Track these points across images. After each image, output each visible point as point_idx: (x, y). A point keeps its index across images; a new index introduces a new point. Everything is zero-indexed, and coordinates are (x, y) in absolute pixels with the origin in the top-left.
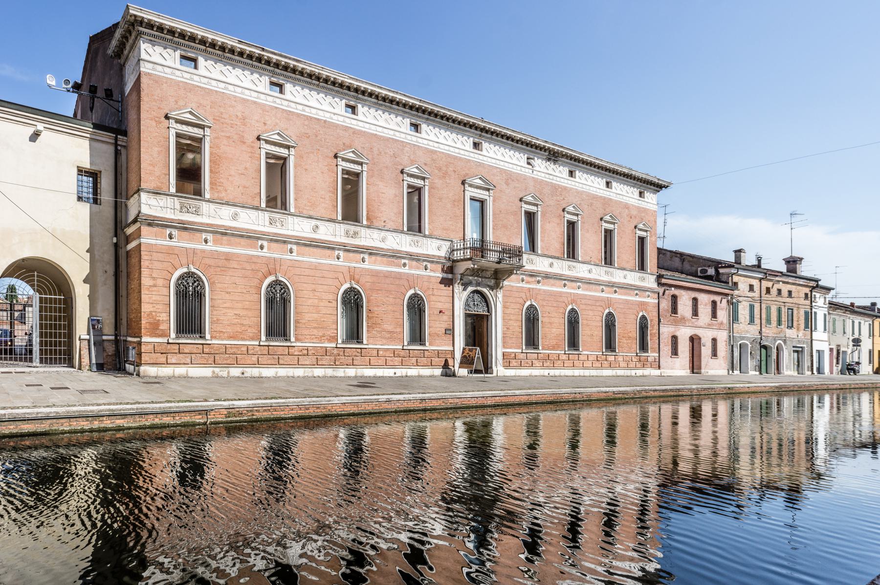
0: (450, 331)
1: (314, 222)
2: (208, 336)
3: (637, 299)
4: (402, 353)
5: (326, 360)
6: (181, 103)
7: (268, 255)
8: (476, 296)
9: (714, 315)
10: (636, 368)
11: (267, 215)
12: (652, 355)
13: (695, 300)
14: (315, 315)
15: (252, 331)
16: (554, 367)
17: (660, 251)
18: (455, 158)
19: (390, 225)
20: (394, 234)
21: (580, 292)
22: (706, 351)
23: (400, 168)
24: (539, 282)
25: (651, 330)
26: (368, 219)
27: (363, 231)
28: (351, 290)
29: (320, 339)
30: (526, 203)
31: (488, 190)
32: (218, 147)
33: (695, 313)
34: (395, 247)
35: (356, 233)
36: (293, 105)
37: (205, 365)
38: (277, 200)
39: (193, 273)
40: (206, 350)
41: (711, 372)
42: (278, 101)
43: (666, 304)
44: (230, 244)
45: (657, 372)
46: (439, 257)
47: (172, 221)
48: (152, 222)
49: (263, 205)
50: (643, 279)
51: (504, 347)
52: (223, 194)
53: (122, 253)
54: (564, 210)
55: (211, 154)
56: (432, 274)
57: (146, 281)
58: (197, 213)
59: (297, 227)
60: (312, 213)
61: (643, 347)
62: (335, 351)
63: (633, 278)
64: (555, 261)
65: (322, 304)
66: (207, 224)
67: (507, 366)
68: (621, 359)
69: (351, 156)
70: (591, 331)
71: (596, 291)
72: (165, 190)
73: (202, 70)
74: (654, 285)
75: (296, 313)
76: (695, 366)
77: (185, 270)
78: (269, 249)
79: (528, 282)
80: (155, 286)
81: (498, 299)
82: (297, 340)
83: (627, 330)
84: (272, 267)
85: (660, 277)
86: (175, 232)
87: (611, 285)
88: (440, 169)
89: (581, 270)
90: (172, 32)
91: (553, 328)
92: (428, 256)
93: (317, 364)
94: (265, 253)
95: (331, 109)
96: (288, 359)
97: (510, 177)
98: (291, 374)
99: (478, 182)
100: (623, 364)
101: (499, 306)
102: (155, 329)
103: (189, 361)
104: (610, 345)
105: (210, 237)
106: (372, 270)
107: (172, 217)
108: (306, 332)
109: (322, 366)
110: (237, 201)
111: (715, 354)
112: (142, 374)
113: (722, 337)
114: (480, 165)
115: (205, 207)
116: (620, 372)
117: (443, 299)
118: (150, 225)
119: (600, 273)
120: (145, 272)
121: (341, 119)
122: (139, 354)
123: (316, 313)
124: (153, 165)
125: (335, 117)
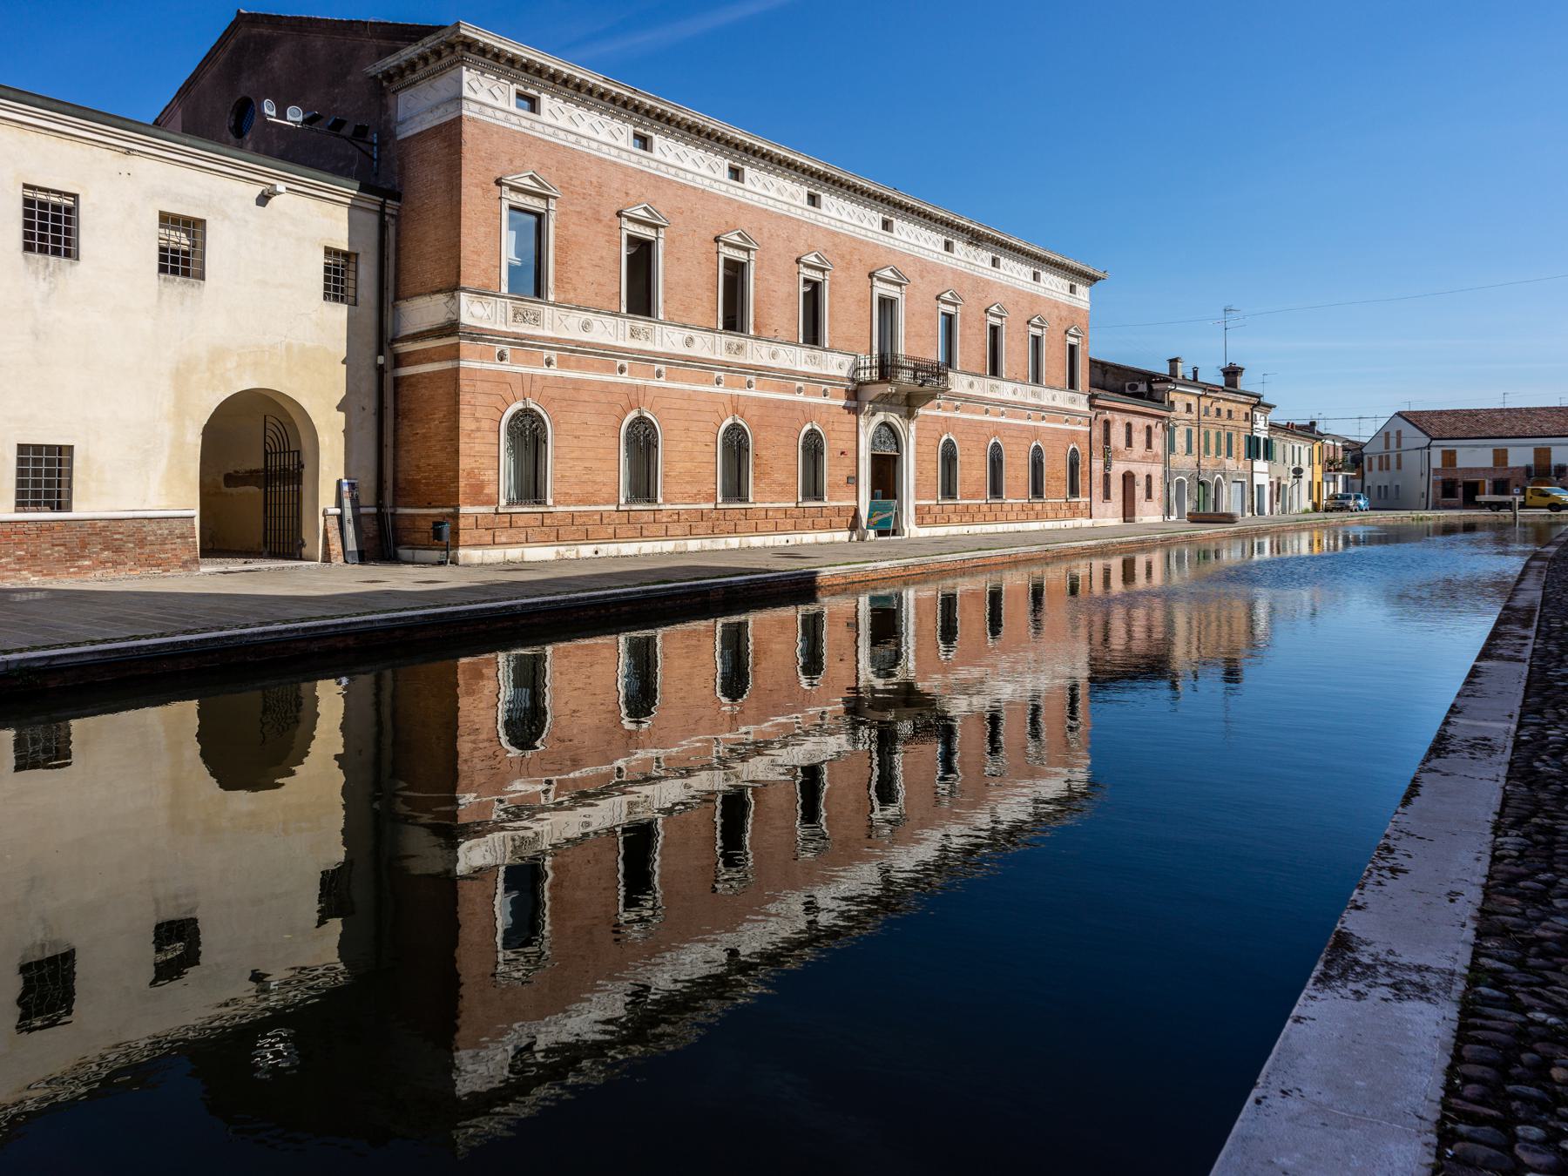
0: (854, 480)
1: (687, 333)
2: (550, 501)
3: (1067, 427)
4: (796, 512)
5: (703, 527)
6: (517, 163)
7: (629, 381)
8: (884, 430)
9: (1149, 445)
10: (1065, 518)
11: (628, 323)
12: (1083, 500)
13: (1129, 425)
14: (689, 465)
15: (606, 491)
16: (973, 522)
17: (1093, 363)
18: (862, 242)
19: (783, 335)
20: (788, 348)
21: (1003, 420)
22: (1140, 491)
23: (796, 256)
24: (957, 408)
25: (1083, 468)
26: (756, 327)
27: (749, 344)
28: (735, 427)
29: (695, 498)
30: (944, 302)
31: (900, 285)
32: (566, 227)
33: (1129, 443)
34: (787, 365)
35: (740, 347)
36: (663, 167)
37: (545, 542)
38: (641, 301)
39: (532, 410)
40: (548, 521)
41: (1147, 520)
42: (645, 161)
43: (1098, 433)
44: (579, 366)
45: (1087, 523)
46: (842, 378)
47: (506, 335)
48: (477, 335)
49: (624, 310)
50: (1073, 401)
51: (917, 498)
52: (571, 295)
53: (388, 378)
54: (986, 311)
55: (557, 236)
56: (832, 402)
57: (466, 424)
58: (536, 320)
59: (665, 338)
60: (685, 320)
61: (1074, 491)
62: (714, 515)
63: (1062, 399)
64: (975, 380)
65: (697, 448)
66: (552, 339)
67: (921, 522)
68: (1048, 507)
69: (735, 239)
70: (1016, 472)
71: (1021, 418)
72: (494, 288)
73: (545, 116)
74: (1086, 409)
75: (665, 462)
76: (1128, 512)
77: (519, 405)
78: (630, 373)
79: (945, 410)
80: (478, 430)
81: (910, 433)
82: (666, 501)
83: (1055, 468)
84: (634, 396)
85: (1092, 398)
86: (507, 349)
87: (1040, 408)
88: (842, 257)
89: (1006, 390)
90: (512, 61)
91: (972, 470)
92: (828, 377)
93: (691, 534)
94: (624, 378)
95: (709, 174)
96: (653, 528)
97: (925, 268)
98: (658, 550)
99: (887, 274)
100: (1051, 514)
101: (912, 441)
102: (478, 496)
103: (523, 537)
104: (1037, 491)
105: (554, 355)
106: (759, 399)
107: (504, 329)
108: (676, 489)
109: (697, 536)
110: (589, 303)
111: (1149, 496)
112: (461, 561)
113: (1157, 471)
114: (890, 251)
115: (547, 311)
116: (1049, 525)
117: (844, 436)
118: (473, 339)
119: (1024, 393)
120: (465, 410)
121: (724, 187)
122: (455, 532)
123: (688, 461)
124: (477, 253)
125: (716, 185)
